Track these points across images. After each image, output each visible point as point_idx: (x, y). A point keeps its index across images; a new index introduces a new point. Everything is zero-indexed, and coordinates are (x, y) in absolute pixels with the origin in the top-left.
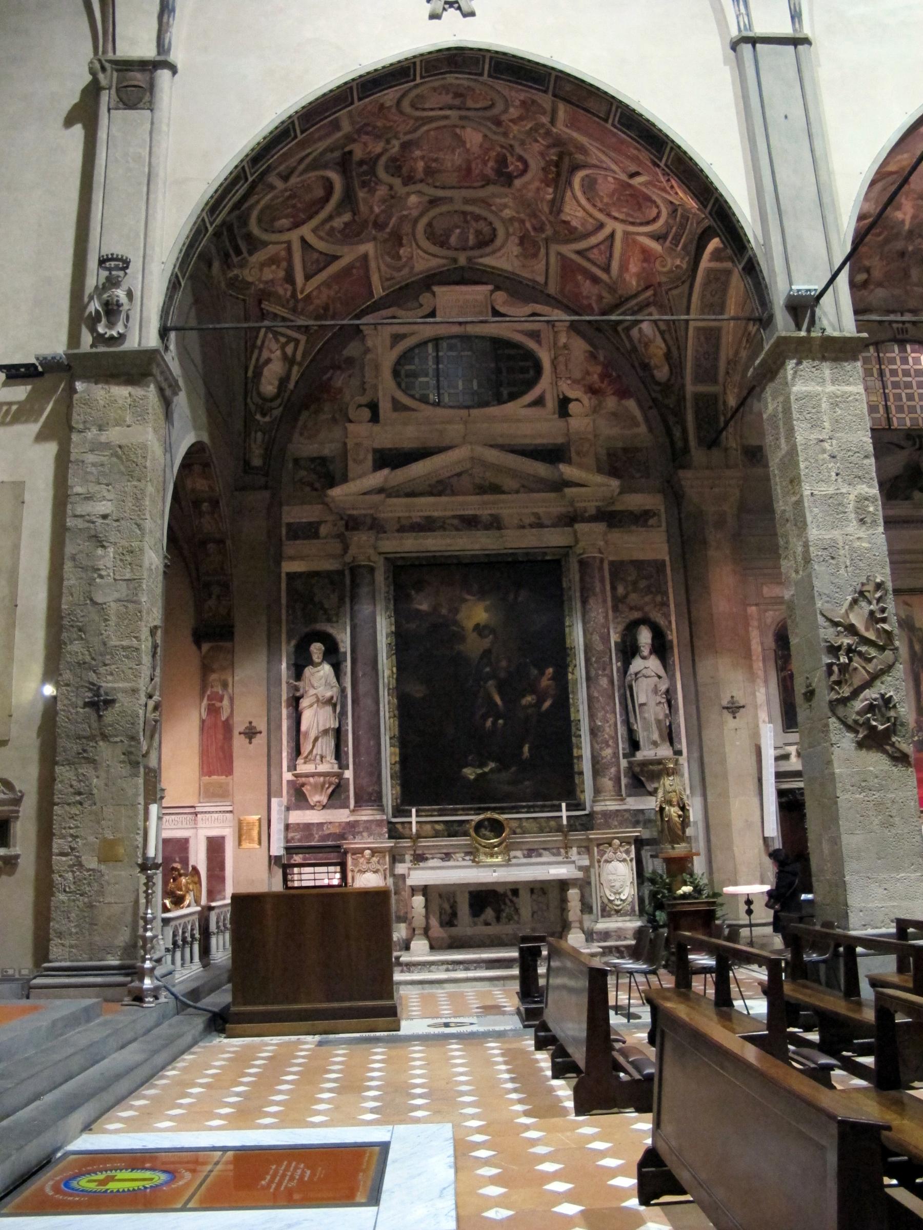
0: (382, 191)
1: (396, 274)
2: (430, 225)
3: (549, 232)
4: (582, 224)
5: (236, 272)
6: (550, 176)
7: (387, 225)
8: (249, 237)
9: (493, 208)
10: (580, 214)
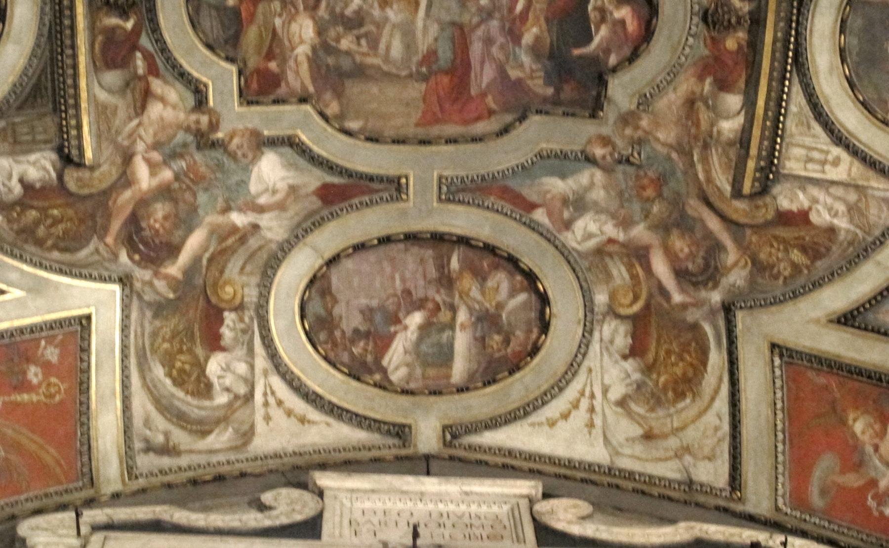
0: (169, 106)
1: (180, 437)
2: (318, 284)
3: (737, 277)
4: (852, 210)
6: (731, 44)
7: (174, 250)
9: (540, 215)
10: (845, 168)
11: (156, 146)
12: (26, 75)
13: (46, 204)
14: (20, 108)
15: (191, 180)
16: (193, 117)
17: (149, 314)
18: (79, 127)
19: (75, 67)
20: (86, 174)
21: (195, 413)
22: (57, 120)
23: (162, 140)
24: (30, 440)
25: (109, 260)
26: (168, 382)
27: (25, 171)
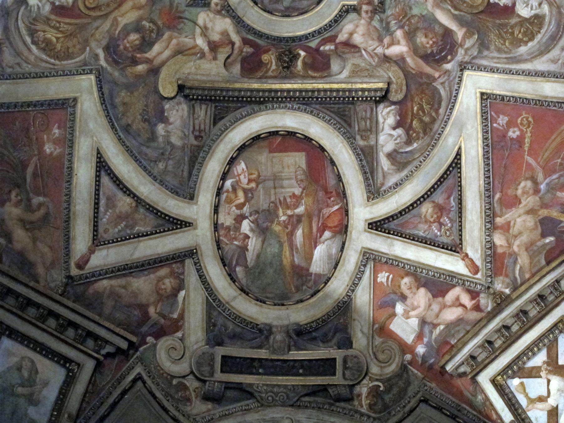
0: (355, 29)
5: (363, 390)
7: (448, 32)
8: (302, 334)
11: (380, 40)
12: (329, 121)
13: (410, 113)
14: (350, 125)
15: (404, 17)
16: (364, 14)
17: (486, 53)
18: (363, 90)
19: (325, 90)
20: (393, 87)
21: (553, 27)
22: (359, 103)
23: (377, 35)
24: (554, 141)
25: (449, 76)
26: (530, 44)
27: (389, 125)
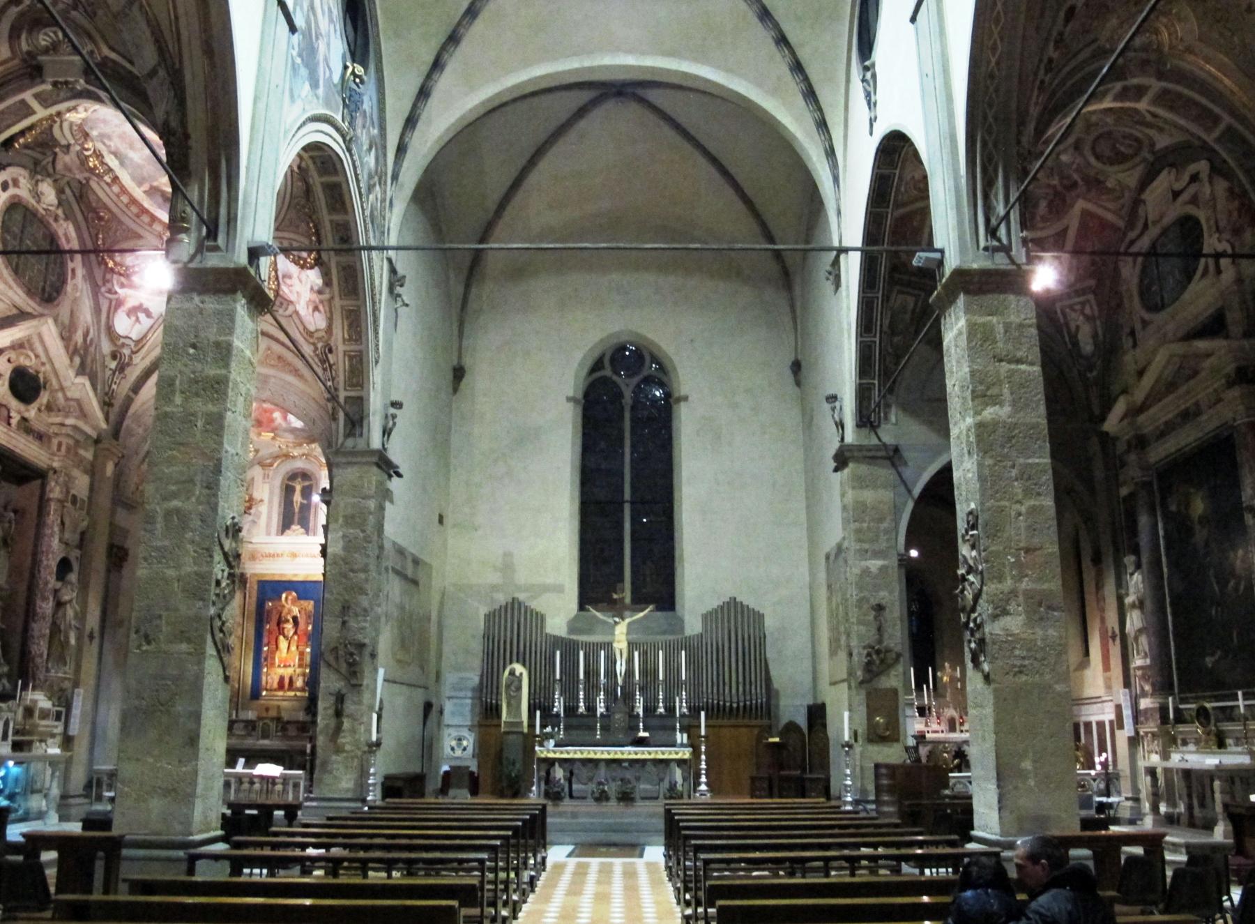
1: (1121, 201)
2: (1098, 157)
